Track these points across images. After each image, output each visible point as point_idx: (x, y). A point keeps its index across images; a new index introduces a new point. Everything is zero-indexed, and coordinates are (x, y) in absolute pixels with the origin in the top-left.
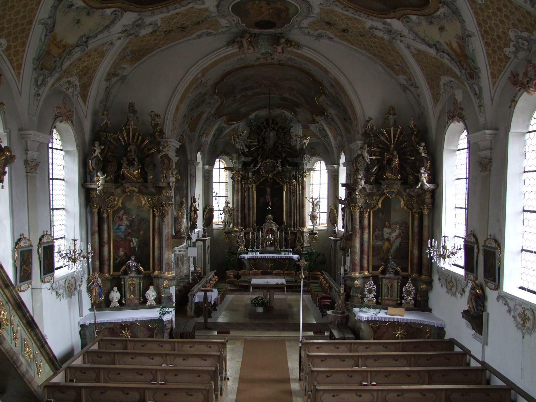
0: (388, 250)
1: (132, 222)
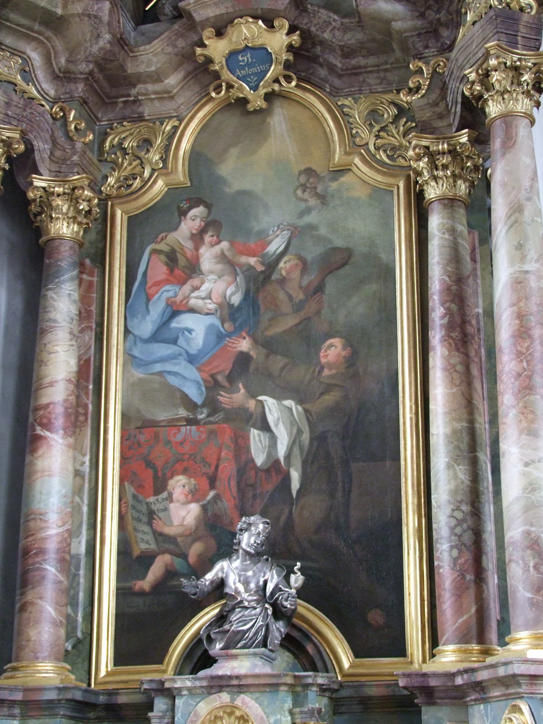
1: (260, 282)
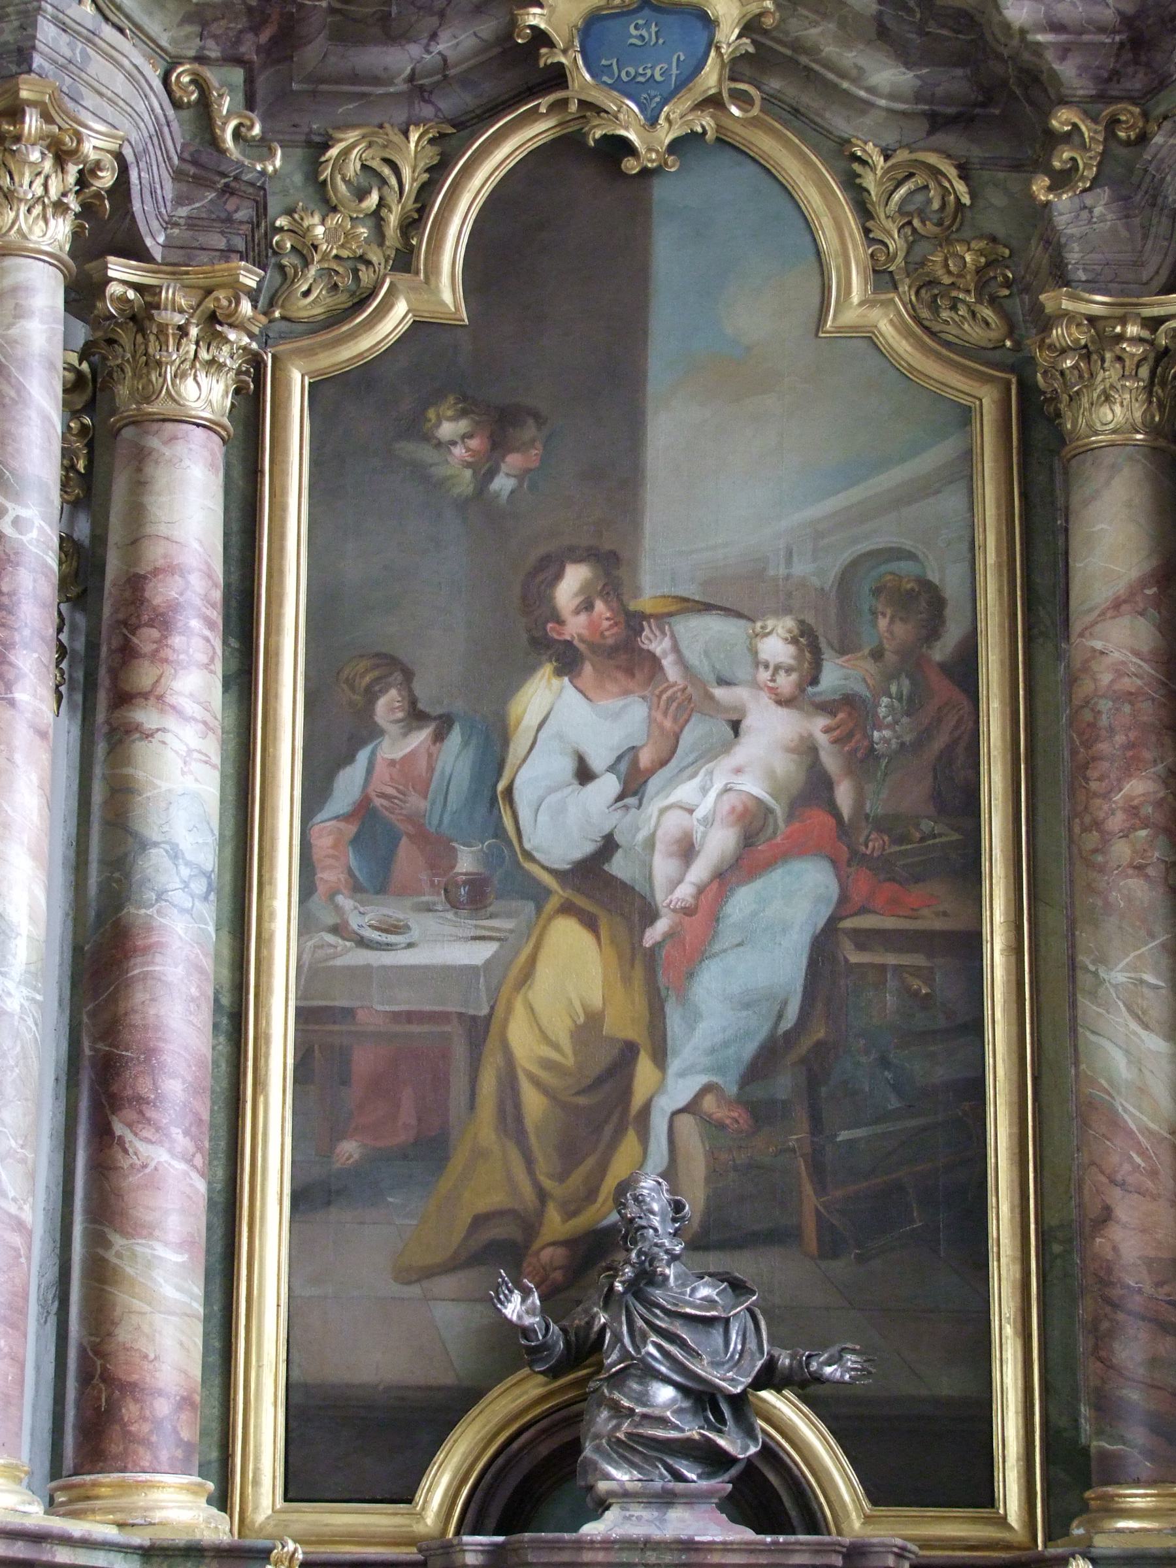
0: (603, 1096)
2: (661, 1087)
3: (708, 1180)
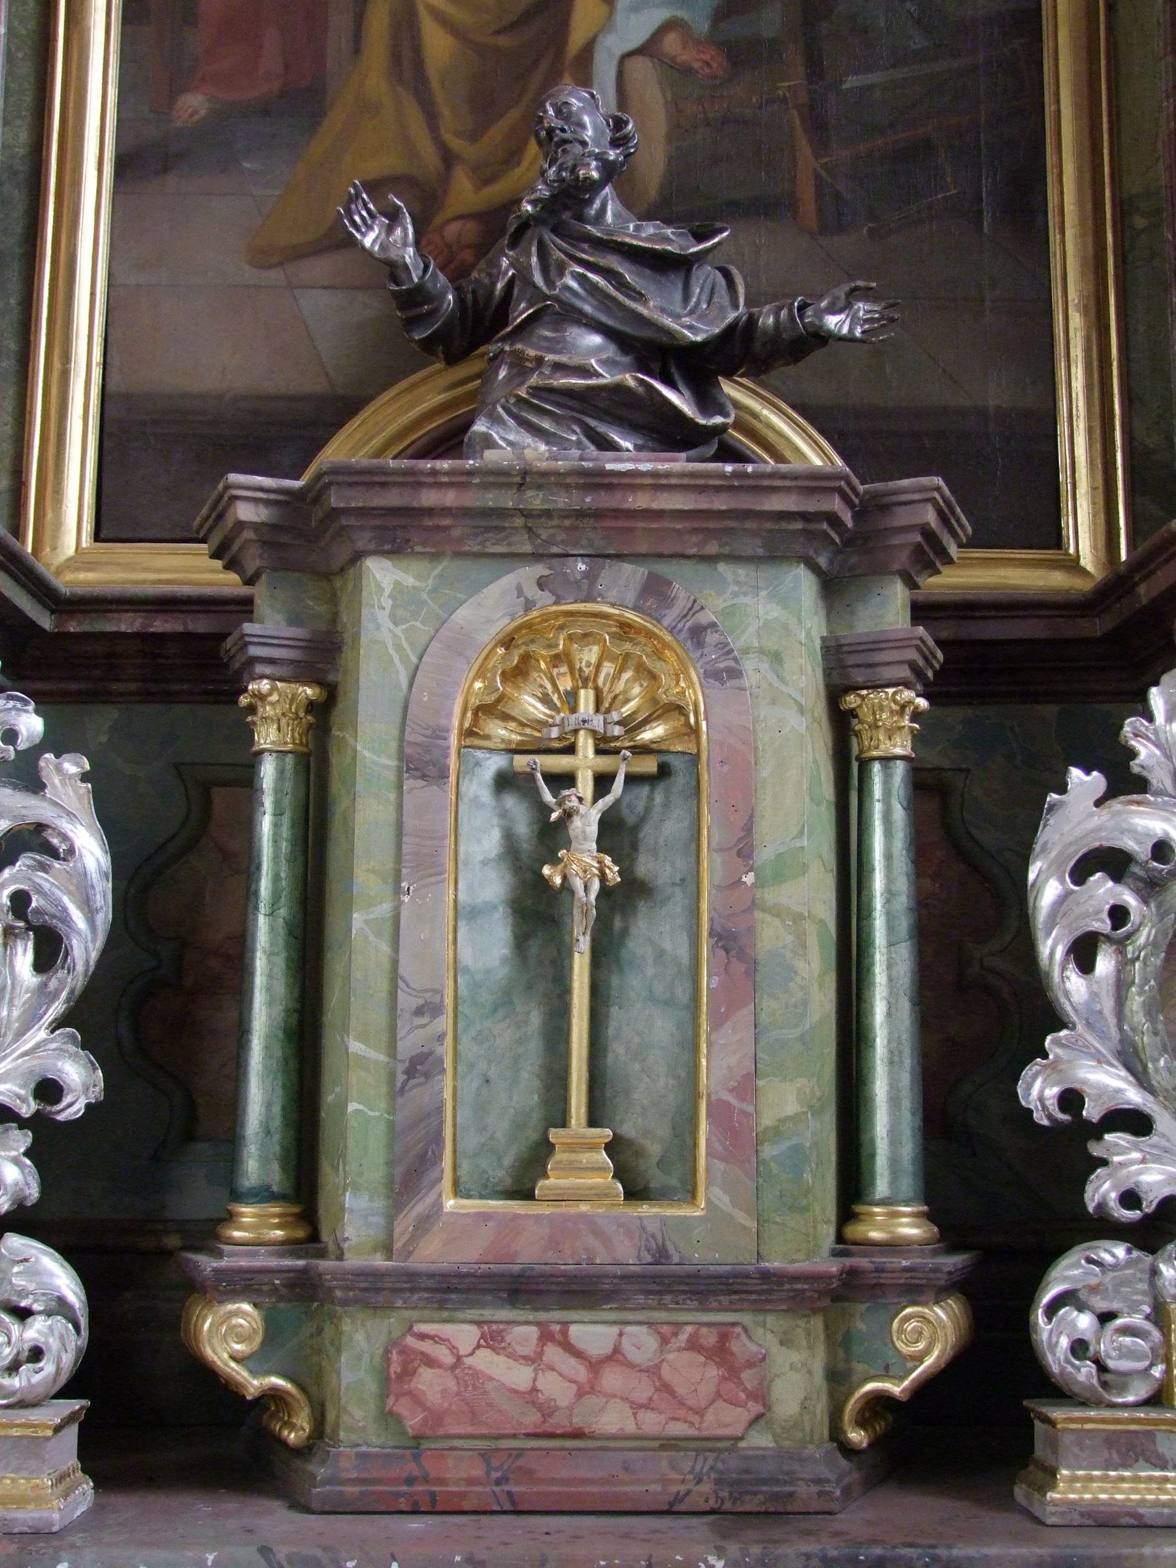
2: (607, 25)
3: (669, 138)
